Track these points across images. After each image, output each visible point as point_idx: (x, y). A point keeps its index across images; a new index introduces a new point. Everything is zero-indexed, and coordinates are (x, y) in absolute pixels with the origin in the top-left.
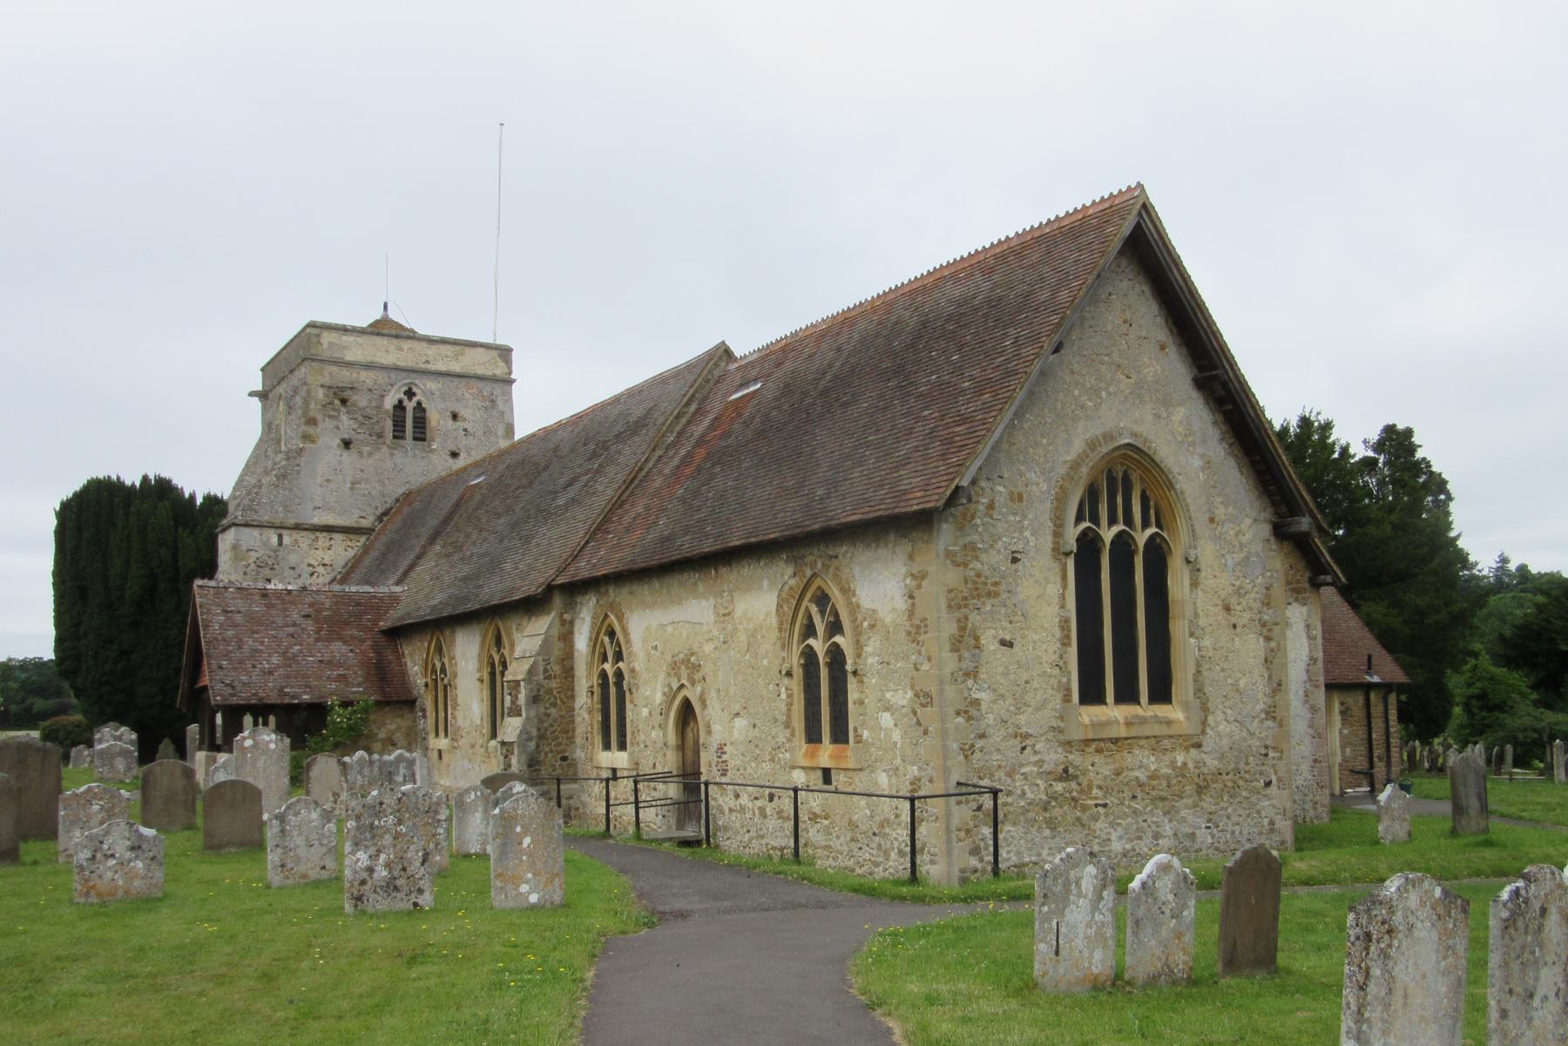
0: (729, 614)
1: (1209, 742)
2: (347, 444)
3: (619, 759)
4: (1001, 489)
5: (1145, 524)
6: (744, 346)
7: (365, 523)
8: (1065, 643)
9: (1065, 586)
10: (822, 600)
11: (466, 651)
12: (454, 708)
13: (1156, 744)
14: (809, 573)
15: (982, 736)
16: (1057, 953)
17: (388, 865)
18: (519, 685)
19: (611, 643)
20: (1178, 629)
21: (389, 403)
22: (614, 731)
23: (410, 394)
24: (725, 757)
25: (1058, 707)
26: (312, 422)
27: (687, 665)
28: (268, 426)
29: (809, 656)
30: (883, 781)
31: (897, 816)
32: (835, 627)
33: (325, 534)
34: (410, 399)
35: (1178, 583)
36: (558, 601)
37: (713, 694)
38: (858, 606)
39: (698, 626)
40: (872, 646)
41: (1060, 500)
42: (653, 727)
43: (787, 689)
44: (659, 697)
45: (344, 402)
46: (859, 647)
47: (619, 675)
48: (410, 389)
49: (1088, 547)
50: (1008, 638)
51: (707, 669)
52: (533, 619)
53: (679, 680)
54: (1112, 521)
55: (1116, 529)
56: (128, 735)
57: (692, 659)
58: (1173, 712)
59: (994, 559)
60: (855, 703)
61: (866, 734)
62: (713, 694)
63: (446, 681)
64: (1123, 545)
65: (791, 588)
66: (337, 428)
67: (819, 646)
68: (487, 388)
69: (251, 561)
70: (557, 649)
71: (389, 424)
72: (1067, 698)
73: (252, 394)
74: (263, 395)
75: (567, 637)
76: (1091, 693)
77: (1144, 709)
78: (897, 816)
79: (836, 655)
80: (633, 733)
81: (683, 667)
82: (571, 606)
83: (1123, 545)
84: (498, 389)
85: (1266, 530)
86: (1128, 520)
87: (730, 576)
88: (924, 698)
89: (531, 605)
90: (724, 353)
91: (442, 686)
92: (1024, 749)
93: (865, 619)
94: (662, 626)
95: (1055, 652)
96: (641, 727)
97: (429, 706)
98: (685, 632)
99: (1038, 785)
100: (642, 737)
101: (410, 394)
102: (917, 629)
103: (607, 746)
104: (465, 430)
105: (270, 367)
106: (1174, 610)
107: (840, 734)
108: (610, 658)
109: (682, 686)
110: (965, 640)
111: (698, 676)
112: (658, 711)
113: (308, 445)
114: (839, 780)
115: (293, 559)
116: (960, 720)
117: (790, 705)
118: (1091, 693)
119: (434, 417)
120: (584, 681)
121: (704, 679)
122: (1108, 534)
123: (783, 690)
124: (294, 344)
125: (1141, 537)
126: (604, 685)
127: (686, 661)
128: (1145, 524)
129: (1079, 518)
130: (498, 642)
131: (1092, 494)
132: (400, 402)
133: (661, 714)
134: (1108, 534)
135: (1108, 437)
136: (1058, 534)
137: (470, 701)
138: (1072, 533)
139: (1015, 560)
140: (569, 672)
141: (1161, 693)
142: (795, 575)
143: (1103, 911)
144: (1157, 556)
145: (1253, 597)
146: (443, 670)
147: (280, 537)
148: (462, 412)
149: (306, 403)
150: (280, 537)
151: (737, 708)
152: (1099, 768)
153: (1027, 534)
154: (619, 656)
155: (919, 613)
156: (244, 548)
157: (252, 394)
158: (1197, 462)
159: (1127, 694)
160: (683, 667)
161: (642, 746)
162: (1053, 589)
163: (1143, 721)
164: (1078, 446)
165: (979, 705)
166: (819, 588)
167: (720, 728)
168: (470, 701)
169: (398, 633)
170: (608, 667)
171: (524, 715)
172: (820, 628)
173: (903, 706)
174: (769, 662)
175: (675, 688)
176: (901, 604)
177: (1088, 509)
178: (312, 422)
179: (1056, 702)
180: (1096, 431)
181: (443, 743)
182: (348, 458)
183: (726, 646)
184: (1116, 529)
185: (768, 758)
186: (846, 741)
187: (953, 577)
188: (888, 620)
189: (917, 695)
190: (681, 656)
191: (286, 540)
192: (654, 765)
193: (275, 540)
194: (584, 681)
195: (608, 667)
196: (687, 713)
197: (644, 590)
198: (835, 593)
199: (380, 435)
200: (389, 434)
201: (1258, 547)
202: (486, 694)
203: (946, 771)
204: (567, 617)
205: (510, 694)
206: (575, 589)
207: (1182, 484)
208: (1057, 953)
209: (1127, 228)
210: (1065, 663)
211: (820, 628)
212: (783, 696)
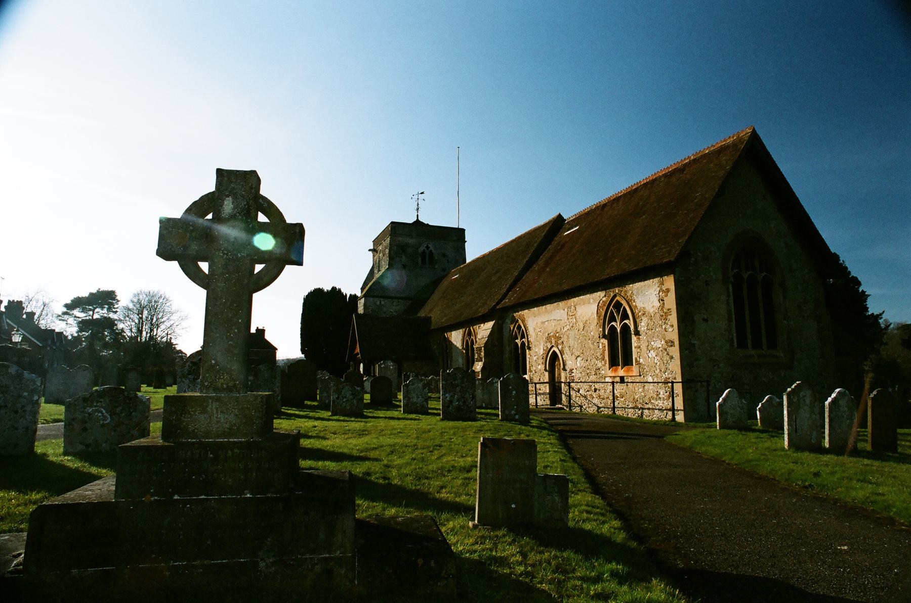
0: (574, 315)
4: (699, 254)
8: (730, 320)
9: (729, 296)
12: (451, 362)
14: (612, 295)
15: (697, 360)
16: (796, 431)
17: (458, 400)
18: (481, 349)
24: (573, 374)
25: (728, 348)
29: (613, 329)
30: (650, 379)
31: (657, 395)
33: (396, 300)
34: (428, 249)
37: (567, 348)
38: (636, 306)
39: (560, 321)
42: (539, 364)
43: (602, 344)
44: (542, 352)
48: (428, 246)
50: (706, 318)
51: (564, 339)
52: (486, 323)
53: (551, 344)
57: (557, 335)
60: (635, 348)
61: (641, 360)
62: (567, 348)
63: (448, 351)
65: (603, 302)
66: (401, 260)
67: (618, 326)
69: (370, 310)
71: (420, 259)
73: (370, 250)
74: (374, 251)
78: (657, 395)
79: (625, 328)
80: (530, 367)
81: (553, 339)
92: (715, 366)
93: (640, 312)
94: (543, 323)
95: (726, 325)
96: (533, 364)
98: (553, 324)
99: (721, 382)
100: (534, 368)
101: (427, 247)
104: (448, 260)
105: (376, 240)
107: (628, 361)
108: (519, 339)
109: (553, 346)
111: (560, 342)
112: (542, 357)
116: (687, 352)
117: (604, 351)
118: (742, 344)
121: (563, 342)
122: (746, 275)
123: (601, 344)
124: (385, 231)
127: (555, 336)
132: (424, 250)
133: (543, 358)
134: (746, 275)
139: (707, 285)
142: (605, 296)
143: (816, 413)
151: (578, 353)
153: (712, 274)
154: (523, 336)
155: (667, 307)
156: (368, 306)
157: (370, 250)
160: (553, 339)
161: (534, 372)
165: (695, 346)
166: (617, 300)
167: (570, 362)
171: (483, 361)
173: (659, 348)
174: (594, 333)
175: (549, 348)
176: (657, 304)
183: (573, 328)
185: (594, 373)
186: (632, 365)
188: (652, 311)
189: (666, 342)
190: (552, 334)
191: (382, 303)
192: (540, 379)
193: (378, 303)
200: (420, 262)
204: (500, 321)
205: (477, 353)
208: (796, 431)
210: (730, 330)
212: (601, 347)
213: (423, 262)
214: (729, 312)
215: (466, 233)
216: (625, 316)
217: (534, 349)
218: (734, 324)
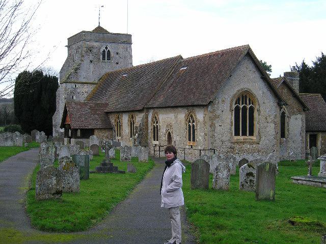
1: (261, 143)
2: (91, 61)
3: (157, 142)
5: (249, 104)
6: (185, 57)
7: (96, 81)
10: (192, 116)
11: (125, 119)
13: (251, 143)
19: (155, 120)
20: (255, 123)
21: (102, 50)
22: (156, 137)
23: (106, 48)
26: (83, 56)
27: (169, 126)
28: (70, 55)
29: (189, 126)
32: (193, 122)
35: (256, 114)
36: (145, 110)
40: (199, 124)
41: (232, 101)
44: (164, 131)
45: (90, 51)
46: (197, 125)
47: (157, 126)
49: (237, 109)
54: (242, 104)
55: (243, 105)
56: (43, 133)
58: (254, 138)
59: (219, 112)
64: (244, 109)
68: (125, 46)
70: (145, 120)
71: (101, 56)
72: (232, 135)
74: (68, 47)
75: (147, 118)
76: (237, 134)
77: (248, 137)
79: (193, 126)
82: (148, 112)
83: (244, 109)
84: (128, 46)
85: (276, 104)
86: (246, 104)
87: (176, 110)
88: (205, 134)
89: (140, 111)
90: (181, 57)
91: (119, 126)
97: (116, 129)
101: (106, 48)
102: (205, 123)
103: (155, 140)
106: (255, 119)
107: (194, 140)
110: (212, 125)
113: (82, 62)
114: (194, 147)
115: (78, 91)
118: (237, 134)
119: (112, 54)
120: (150, 128)
122: (241, 106)
125: (248, 107)
126: (154, 128)
128: (249, 104)
129: (235, 104)
130: (132, 117)
131: (239, 99)
132: (104, 50)
135: (242, 89)
136: (231, 106)
137: (126, 129)
138: (234, 106)
140: (147, 125)
141: (251, 134)
144: (252, 110)
145: (272, 117)
146: (120, 122)
147: (75, 86)
148: (119, 52)
149: (82, 51)
150: (75, 86)
152: (237, 147)
158: (261, 92)
159: (244, 134)
162: (230, 117)
163: (247, 139)
164: (235, 91)
168: (126, 129)
169: (107, 113)
170: (155, 124)
172: (191, 121)
177: (238, 102)
178: (83, 56)
179: (229, 135)
180: (239, 88)
181: (119, 138)
182: (92, 65)
184: (243, 105)
187: (211, 115)
191: (77, 86)
194: (150, 128)
195: (155, 124)
196: (169, 135)
197: (162, 110)
198: (193, 115)
199: (99, 59)
200: (101, 59)
201: (274, 107)
202: (130, 128)
203: (209, 146)
206: (151, 108)
207: (258, 97)
209: (246, 52)
211: (191, 121)
213: (104, 59)
214: (232, 123)
215: (132, 37)
216: (193, 122)
217: (161, 130)
218: (233, 127)
